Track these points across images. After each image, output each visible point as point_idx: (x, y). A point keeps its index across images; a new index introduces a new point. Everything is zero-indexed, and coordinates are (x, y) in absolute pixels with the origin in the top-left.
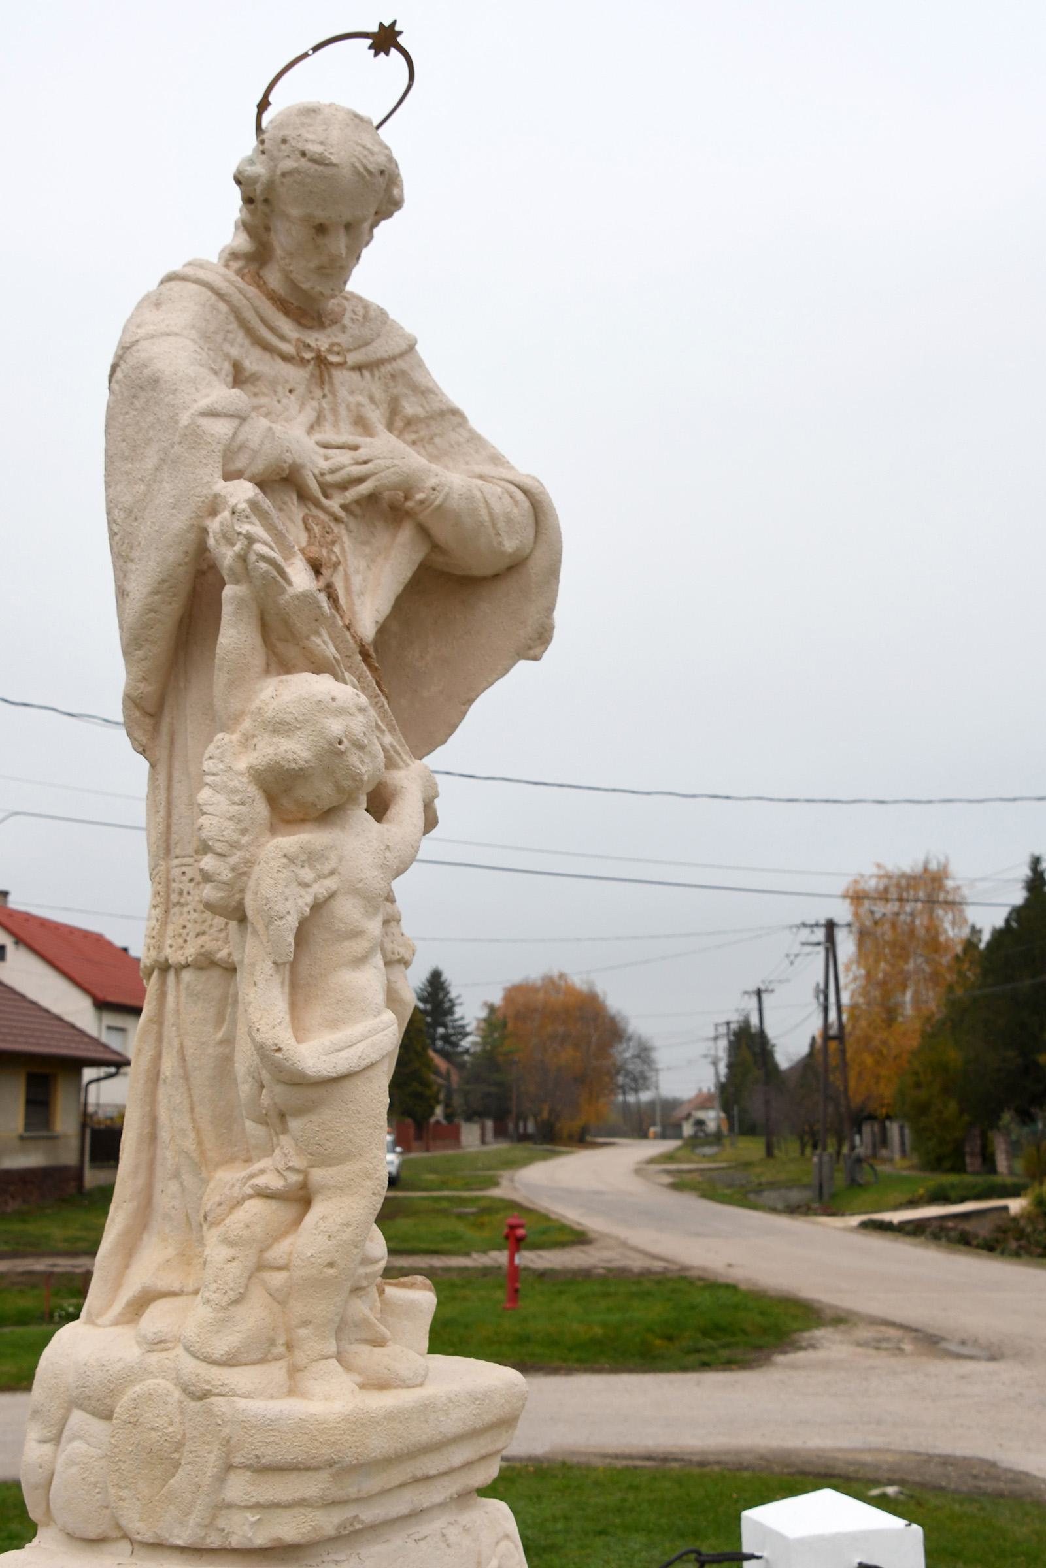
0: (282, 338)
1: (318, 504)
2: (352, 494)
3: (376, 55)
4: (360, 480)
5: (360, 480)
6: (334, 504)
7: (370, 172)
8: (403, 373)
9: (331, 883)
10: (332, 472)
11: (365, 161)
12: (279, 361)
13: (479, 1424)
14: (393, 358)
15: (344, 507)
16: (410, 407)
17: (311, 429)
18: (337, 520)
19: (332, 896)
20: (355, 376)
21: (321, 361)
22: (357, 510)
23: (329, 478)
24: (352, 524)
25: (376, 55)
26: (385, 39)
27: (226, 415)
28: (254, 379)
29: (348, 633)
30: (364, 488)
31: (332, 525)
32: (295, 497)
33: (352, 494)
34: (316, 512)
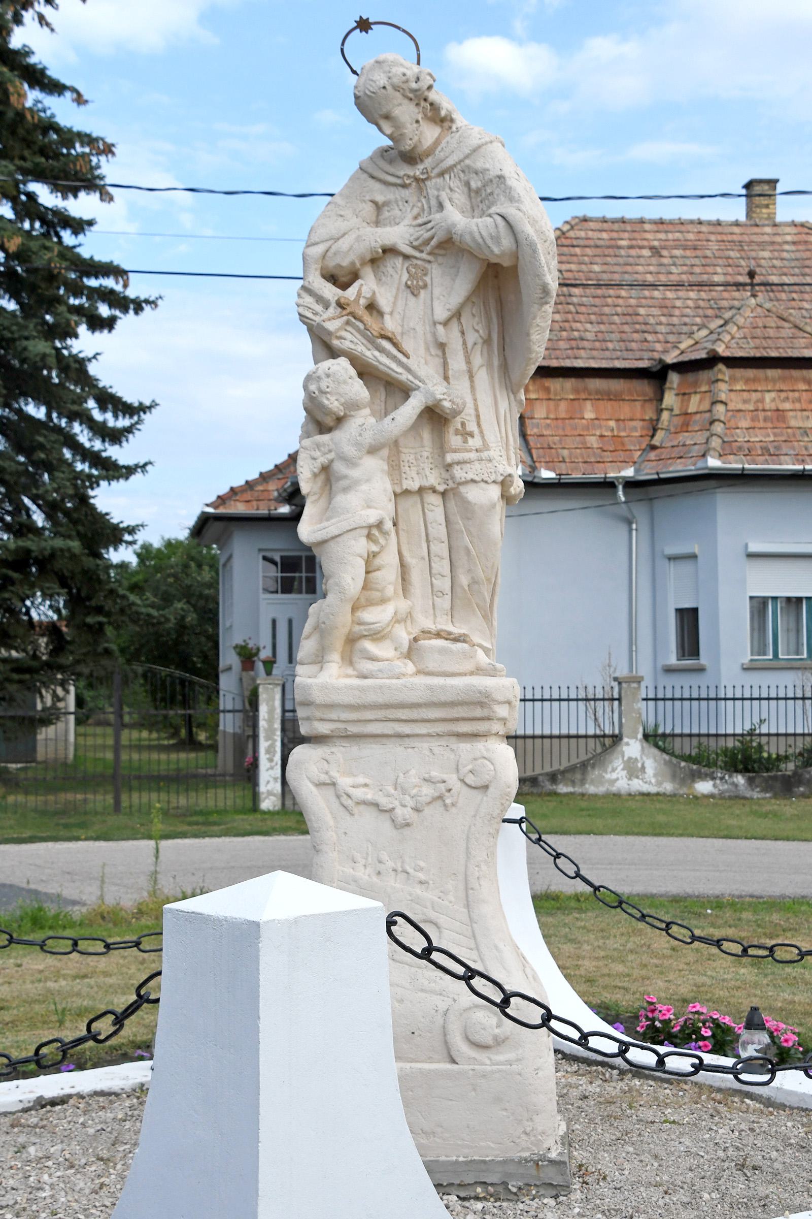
0: (398, 177)
1: (416, 258)
2: (428, 248)
3: (367, 32)
4: (432, 238)
5: (432, 238)
6: (424, 256)
7: (373, 93)
8: (468, 167)
10: (416, 239)
11: (371, 89)
12: (400, 188)
13: (435, 699)
14: (461, 161)
15: (430, 254)
16: (473, 185)
17: (416, 218)
18: (429, 262)
19: (332, 461)
20: (439, 180)
21: (417, 180)
22: (442, 252)
23: (415, 243)
24: (440, 259)
25: (367, 32)
26: (364, 25)
27: (323, 242)
28: (386, 204)
30: (433, 243)
31: (427, 266)
32: (401, 259)
33: (428, 248)
34: (415, 261)
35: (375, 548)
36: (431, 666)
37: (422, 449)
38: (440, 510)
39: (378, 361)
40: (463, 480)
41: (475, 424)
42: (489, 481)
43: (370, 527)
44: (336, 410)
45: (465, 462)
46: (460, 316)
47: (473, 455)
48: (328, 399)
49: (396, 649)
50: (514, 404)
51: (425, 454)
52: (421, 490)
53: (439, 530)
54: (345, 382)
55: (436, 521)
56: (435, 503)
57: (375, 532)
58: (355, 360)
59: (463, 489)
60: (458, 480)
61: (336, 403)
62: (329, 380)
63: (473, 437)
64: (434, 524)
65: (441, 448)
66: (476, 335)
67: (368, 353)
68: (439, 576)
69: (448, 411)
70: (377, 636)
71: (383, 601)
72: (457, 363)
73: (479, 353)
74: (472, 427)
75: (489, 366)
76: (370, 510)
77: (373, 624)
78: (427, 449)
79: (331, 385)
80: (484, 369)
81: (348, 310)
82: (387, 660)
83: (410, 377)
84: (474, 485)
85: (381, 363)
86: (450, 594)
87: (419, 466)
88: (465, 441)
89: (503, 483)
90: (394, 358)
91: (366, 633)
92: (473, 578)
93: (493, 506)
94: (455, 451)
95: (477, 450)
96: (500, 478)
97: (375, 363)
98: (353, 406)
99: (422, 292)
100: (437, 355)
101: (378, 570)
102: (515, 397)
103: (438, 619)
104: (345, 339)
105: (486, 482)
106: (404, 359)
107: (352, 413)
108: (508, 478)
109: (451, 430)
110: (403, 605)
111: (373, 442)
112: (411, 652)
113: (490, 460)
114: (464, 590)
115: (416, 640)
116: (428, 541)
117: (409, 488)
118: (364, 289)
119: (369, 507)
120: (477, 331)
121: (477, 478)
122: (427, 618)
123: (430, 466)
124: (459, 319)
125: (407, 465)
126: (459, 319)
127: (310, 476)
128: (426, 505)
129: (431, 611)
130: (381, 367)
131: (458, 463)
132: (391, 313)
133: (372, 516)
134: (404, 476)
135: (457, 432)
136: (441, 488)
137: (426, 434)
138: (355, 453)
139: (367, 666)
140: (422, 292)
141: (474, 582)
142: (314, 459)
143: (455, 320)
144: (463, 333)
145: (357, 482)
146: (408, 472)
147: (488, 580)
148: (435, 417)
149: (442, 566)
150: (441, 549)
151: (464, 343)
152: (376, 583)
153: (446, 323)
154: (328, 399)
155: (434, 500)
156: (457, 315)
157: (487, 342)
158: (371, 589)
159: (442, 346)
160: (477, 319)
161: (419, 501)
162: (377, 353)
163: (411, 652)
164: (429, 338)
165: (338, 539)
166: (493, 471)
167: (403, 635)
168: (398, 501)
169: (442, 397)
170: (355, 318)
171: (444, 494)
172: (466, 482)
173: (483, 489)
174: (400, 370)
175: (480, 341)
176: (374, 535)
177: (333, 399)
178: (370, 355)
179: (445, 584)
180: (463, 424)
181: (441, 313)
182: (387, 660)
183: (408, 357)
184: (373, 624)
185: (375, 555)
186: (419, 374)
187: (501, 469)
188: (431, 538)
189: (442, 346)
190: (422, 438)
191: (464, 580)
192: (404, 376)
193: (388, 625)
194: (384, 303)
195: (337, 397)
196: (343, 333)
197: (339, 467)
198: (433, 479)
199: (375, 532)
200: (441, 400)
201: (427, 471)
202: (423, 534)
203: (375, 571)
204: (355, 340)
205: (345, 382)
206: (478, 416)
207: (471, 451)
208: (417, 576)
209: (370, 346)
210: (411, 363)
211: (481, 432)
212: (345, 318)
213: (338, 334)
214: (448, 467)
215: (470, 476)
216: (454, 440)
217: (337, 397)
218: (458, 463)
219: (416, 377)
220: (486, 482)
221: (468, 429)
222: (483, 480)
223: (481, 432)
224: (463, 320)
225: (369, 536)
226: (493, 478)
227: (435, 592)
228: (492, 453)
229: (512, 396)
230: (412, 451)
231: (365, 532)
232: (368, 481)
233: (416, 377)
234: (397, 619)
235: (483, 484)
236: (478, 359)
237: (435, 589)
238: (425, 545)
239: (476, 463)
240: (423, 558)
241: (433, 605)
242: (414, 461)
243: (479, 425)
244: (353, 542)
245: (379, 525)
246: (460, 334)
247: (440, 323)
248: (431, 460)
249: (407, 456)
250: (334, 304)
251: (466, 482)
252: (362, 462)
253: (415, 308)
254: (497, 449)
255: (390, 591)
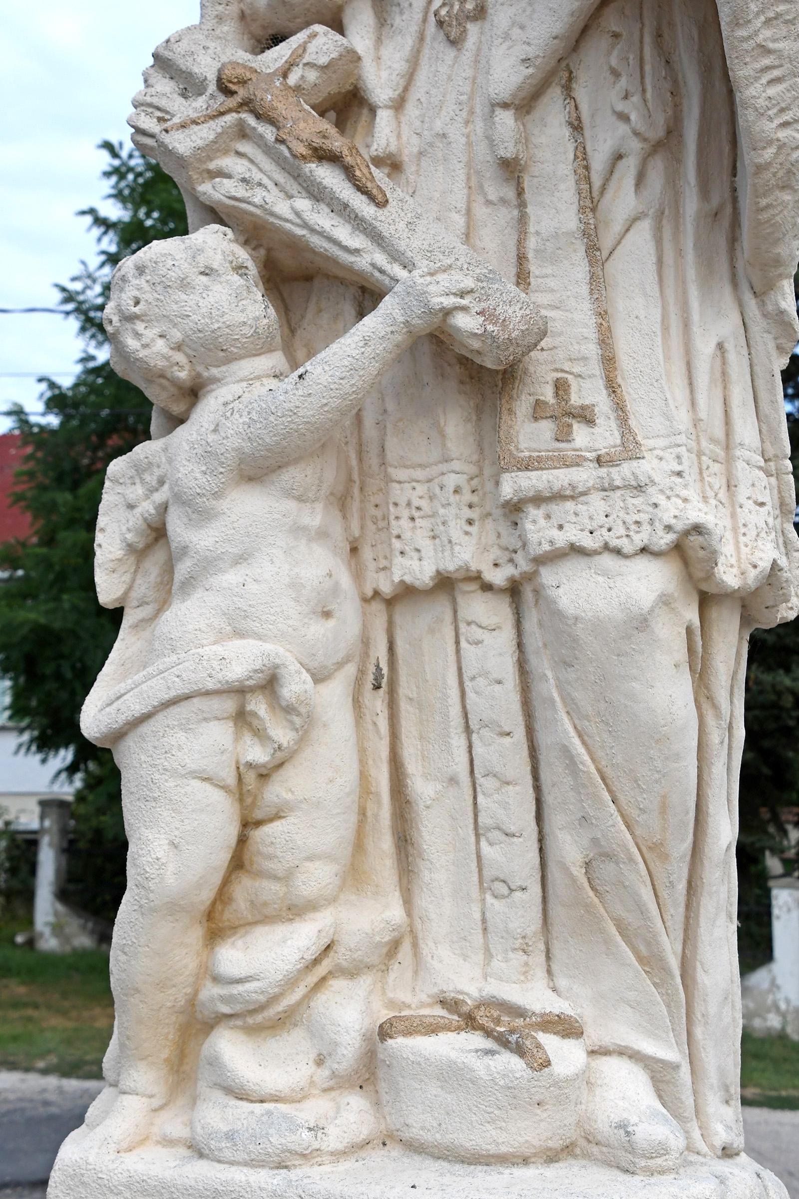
9: (159, 497)
29: (283, 148)
35: (257, 754)
36: (420, 1122)
37: (444, 467)
38: (506, 637)
39: (305, 225)
40: (546, 547)
41: (601, 383)
42: (628, 548)
43: (240, 691)
44: (161, 363)
45: (558, 497)
46: (570, 79)
47: (585, 476)
48: (137, 335)
49: (320, 1061)
50: (758, 325)
51: (451, 481)
52: (445, 584)
53: (499, 700)
54: (184, 285)
55: (485, 674)
56: (485, 622)
57: (259, 706)
58: (253, 231)
59: (548, 576)
60: (535, 550)
61: (160, 346)
62: (142, 282)
63: (590, 421)
64: (481, 681)
65: (493, 457)
66: (623, 129)
67: (282, 208)
68: (496, 835)
69: (476, 344)
70: (264, 1018)
71: (295, 910)
72: (556, 211)
73: (629, 182)
74: (589, 392)
75: (665, 216)
76: (237, 644)
77: (240, 981)
78: (456, 465)
79: (148, 296)
80: (645, 227)
81: (242, 93)
82: (276, 1099)
83: (380, 259)
84: (583, 561)
85: (313, 231)
86: (536, 890)
87: (434, 515)
88: (564, 435)
89: (679, 549)
90: (342, 210)
91: (226, 1009)
92: (595, 841)
93: (641, 623)
94: (527, 466)
95: (599, 460)
96: (665, 540)
97: (300, 232)
98: (213, 351)
99: (473, 29)
100: (503, 201)
101: (277, 817)
102: (762, 304)
103: (496, 964)
104: (229, 176)
105: (618, 552)
106: (366, 209)
107: (214, 371)
108: (695, 540)
109: (523, 406)
110: (370, 917)
111: (247, 447)
112: (369, 1072)
113: (639, 488)
114: (573, 879)
115: (384, 1032)
116: (468, 730)
117: (408, 579)
118: (312, 47)
119: (239, 634)
120: (624, 117)
121: (588, 542)
122: (465, 957)
123: (467, 513)
124: (568, 89)
125: (405, 513)
126: (568, 89)
127: (119, 554)
128: (463, 627)
129: (478, 938)
130: (316, 241)
131: (538, 500)
132: (399, 105)
133: (240, 660)
134: (397, 544)
135: (539, 411)
136: (498, 577)
137: (455, 425)
138: (202, 480)
139: (217, 1115)
140: (473, 29)
141: (599, 857)
142: (131, 507)
143: (555, 93)
144: (577, 127)
145: (209, 564)
146: (407, 535)
147: (653, 851)
148: (473, 375)
149: (512, 806)
150: (506, 754)
151: (582, 157)
152: (270, 857)
153: (525, 103)
154: (137, 335)
155: (481, 609)
156: (558, 72)
157: (667, 143)
158: (260, 874)
159: (511, 169)
160: (623, 82)
161: (448, 617)
162: (303, 204)
163: (369, 1072)
164: (482, 151)
165: (145, 729)
166: (643, 517)
167: (347, 1012)
168: (398, 619)
169: (449, 302)
170: (258, 117)
171: (514, 590)
172: (556, 556)
173: (607, 574)
174: (356, 241)
175: (635, 146)
176: (254, 714)
177: (150, 334)
178: (288, 208)
179: (517, 859)
180: (561, 387)
181: (507, 73)
182: (276, 1099)
183: (382, 204)
184: (240, 981)
185: (264, 775)
186: (402, 246)
187: (670, 511)
188: (474, 724)
189: (511, 169)
190: (443, 435)
191: (569, 849)
192: (369, 258)
193: (291, 982)
194: (380, 83)
195: (163, 327)
196: (227, 162)
197: (176, 526)
198: (468, 551)
199: (259, 706)
200: (447, 312)
201: (456, 530)
202: (455, 711)
203: (271, 820)
204: (257, 176)
205: (184, 285)
206: (609, 362)
207: (577, 462)
208: (437, 833)
209: (293, 187)
210: (387, 220)
211: (620, 408)
212: (230, 118)
213: (212, 166)
214: (514, 510)
215: (573, 535)
216: (530, 435)
217: (163, 327)
218: (538, 500)
219: (396, 256)
220: (618, 552)
221: (575, 400)
222: (607, 547)
223: (620, 408)
224: (581, 93)
225: (242, 718)
226: (640, 539)
227: (489, 882)
228: (646, 467)
229: (751, 304)
230: (419, 474)
231: (229, 705)
232: (240, 559)
233: (396, 256)
234: (325, 964)
235: (607, 560)
236: (623, 200)
237: (488, 873)
238: (458, 742)
239: (595, 499)
240: (453, 780)
241: (484, 921)
242: (424, 503)
243: (612, 387)
244: (181, 736)
245: (270, 683)
246: (567, 132)
247: (505, 106)
248: (467, 497)
249: (407, 491)
250: (212, 88)
251: (556, 556)
252: (223, 505)
253: (446, 76)
254: (669, 455)
255: (317, 878)
